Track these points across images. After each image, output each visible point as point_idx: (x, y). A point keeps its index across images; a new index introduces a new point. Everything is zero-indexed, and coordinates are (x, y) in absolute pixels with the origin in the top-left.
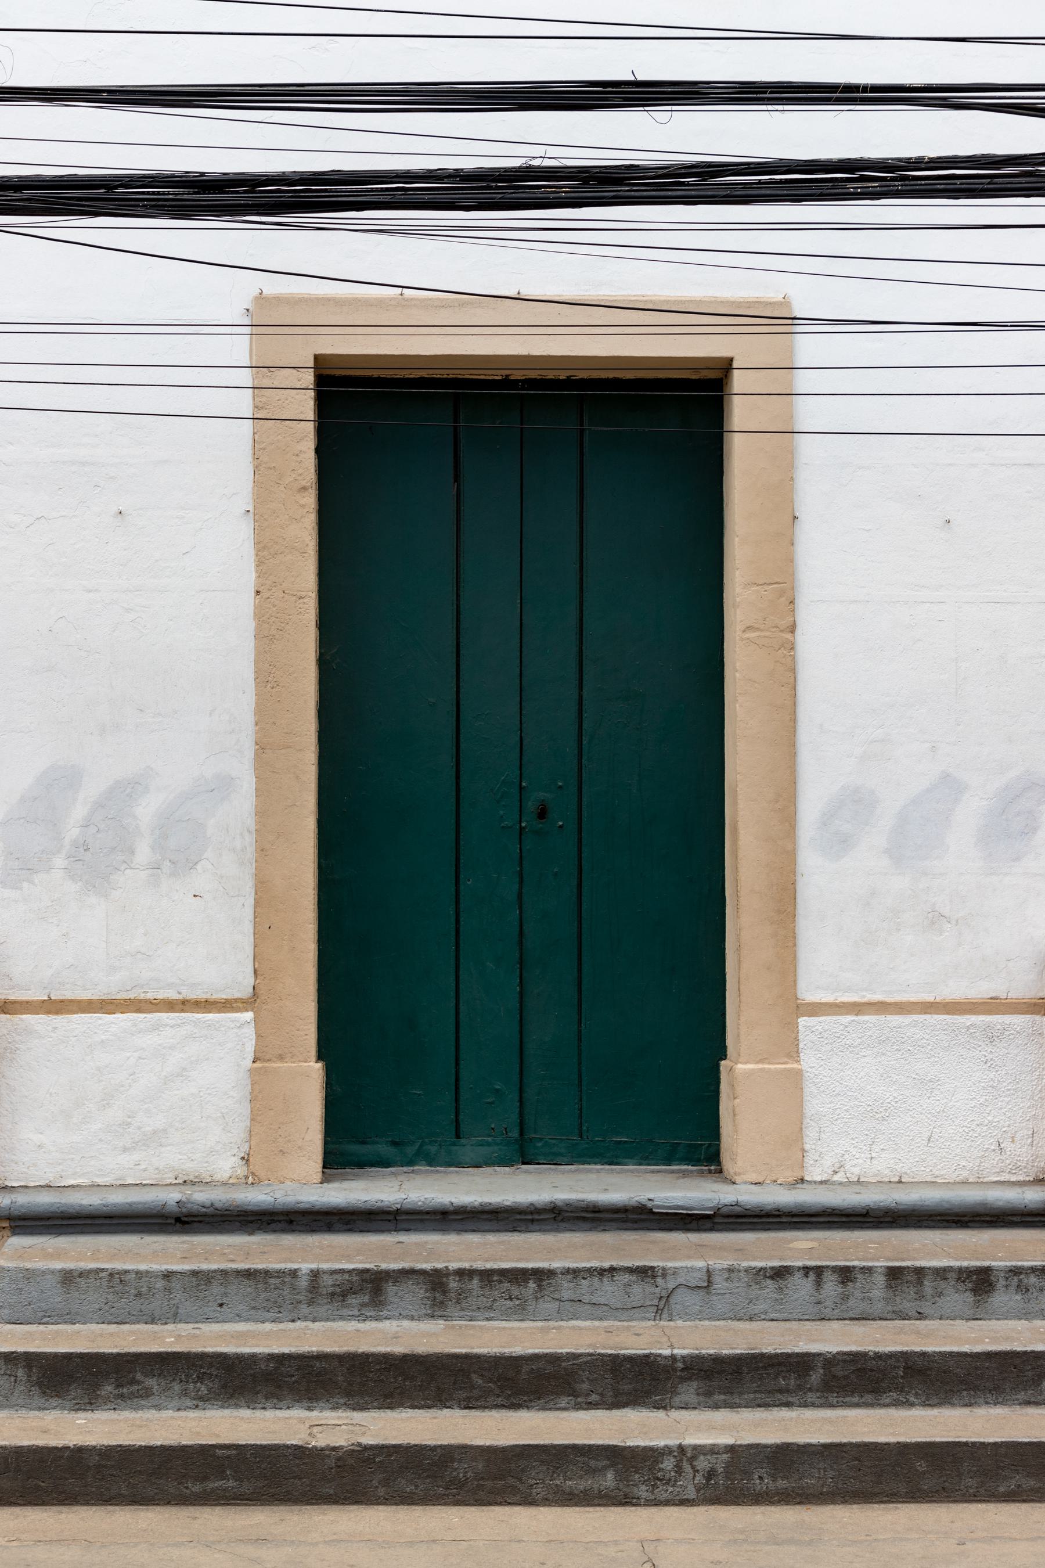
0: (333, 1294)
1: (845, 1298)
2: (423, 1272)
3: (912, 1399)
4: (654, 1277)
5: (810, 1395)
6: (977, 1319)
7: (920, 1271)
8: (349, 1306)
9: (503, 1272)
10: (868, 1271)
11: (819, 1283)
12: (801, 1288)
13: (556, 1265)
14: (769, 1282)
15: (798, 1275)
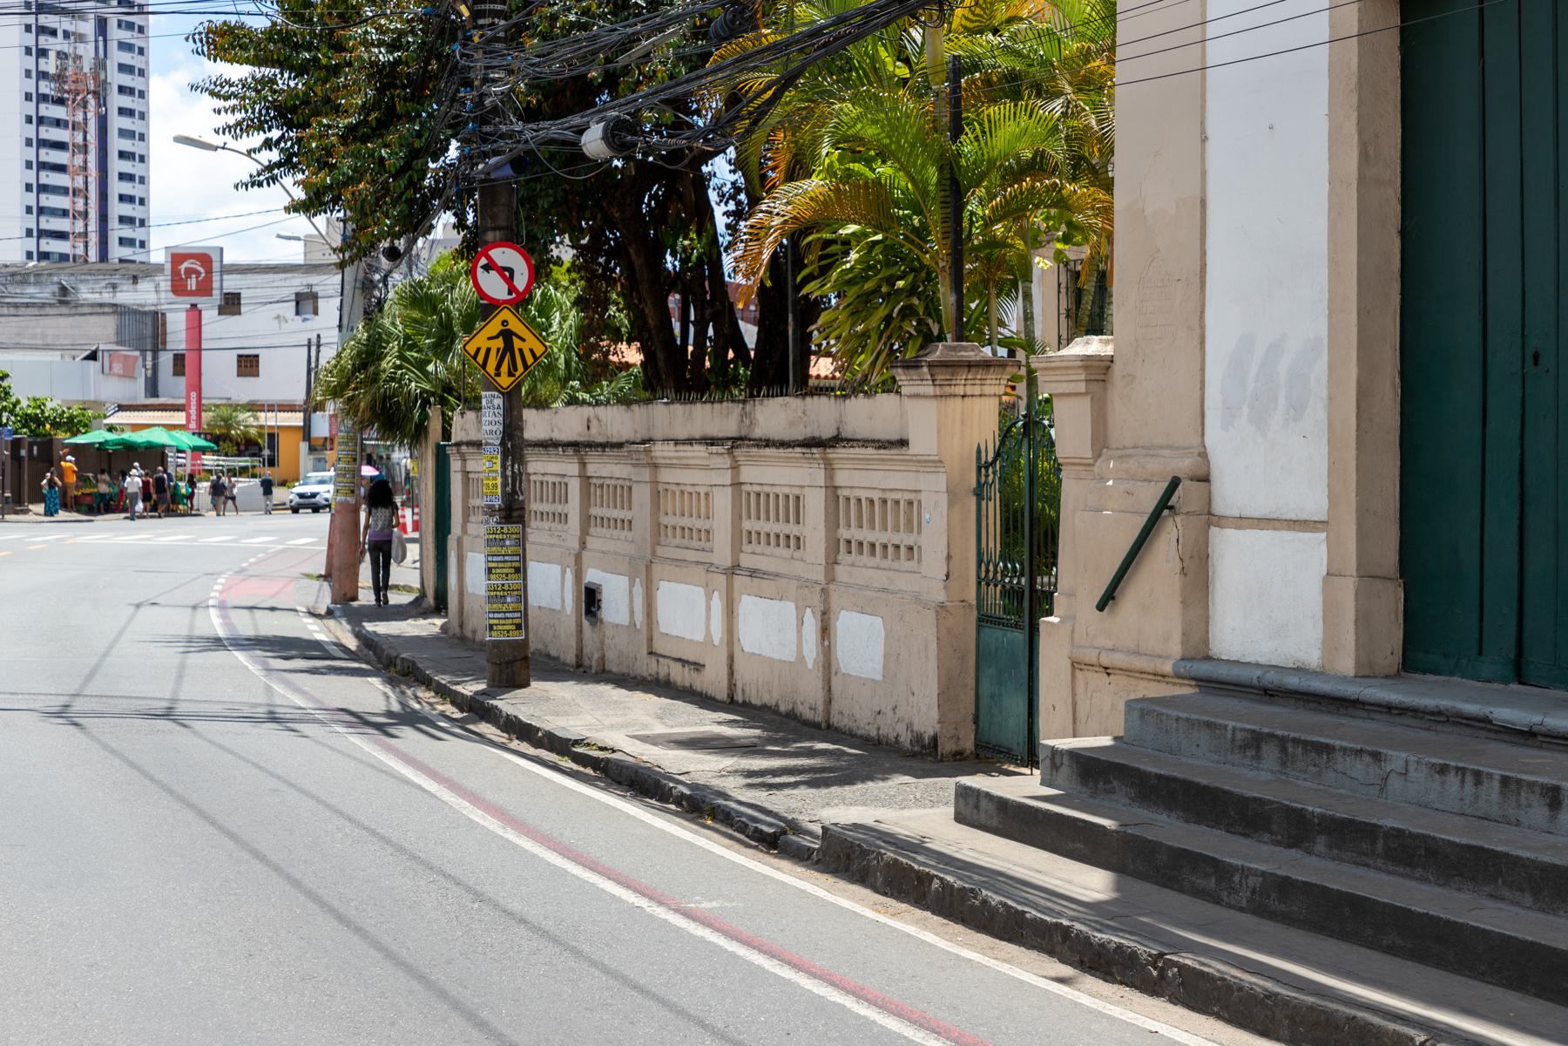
0: (1240, 746)
1: (1476, 798)
2: (1277, 737)
3: (1430, 877)
4: (1380, 761)
5: (1378, 860)
6: (1550, 833)
7: (1519, 782)
8: (1245, 757)
9: (1313, 743)
10: (1490, 776)
11: (1463, 782)
12: (1453, 780)
13: (1337, 743)
14: (1437, 776)
15: (1453, 773)
